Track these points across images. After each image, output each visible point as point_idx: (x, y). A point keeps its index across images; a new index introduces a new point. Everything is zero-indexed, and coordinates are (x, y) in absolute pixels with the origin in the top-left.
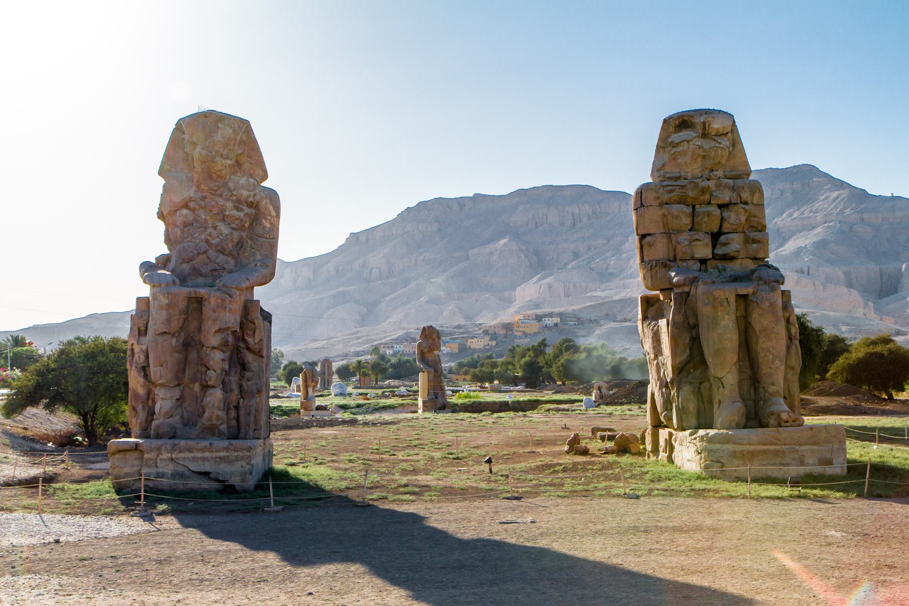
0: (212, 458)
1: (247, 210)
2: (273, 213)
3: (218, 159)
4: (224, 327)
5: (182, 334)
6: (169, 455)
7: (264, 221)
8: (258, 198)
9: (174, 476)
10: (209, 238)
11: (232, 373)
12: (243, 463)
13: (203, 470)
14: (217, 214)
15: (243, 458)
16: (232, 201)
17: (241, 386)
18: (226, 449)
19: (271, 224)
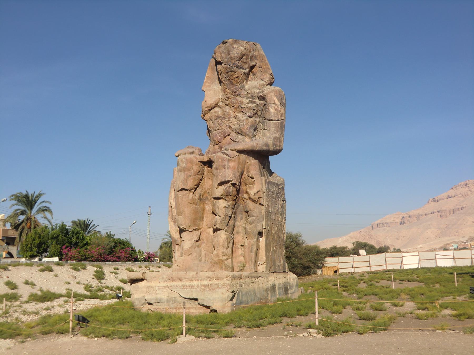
0: (198, 286)
1: (258, 102)
2: (277, 102)
3: (234, 69)
4: (223, 180)
5: (199, 190)
6: (165, 284)
7: (270, 108)
8: (265, 93)
9: (168, 301)
10: (231, 125)
11: (238, 218)
12: (224, 290)
13: (191, 297)
14: (237, 108)
15: (223, 286)
16: (248, 98)
17: (245, 229)
18: (210, 278)
19: (276, 110)
